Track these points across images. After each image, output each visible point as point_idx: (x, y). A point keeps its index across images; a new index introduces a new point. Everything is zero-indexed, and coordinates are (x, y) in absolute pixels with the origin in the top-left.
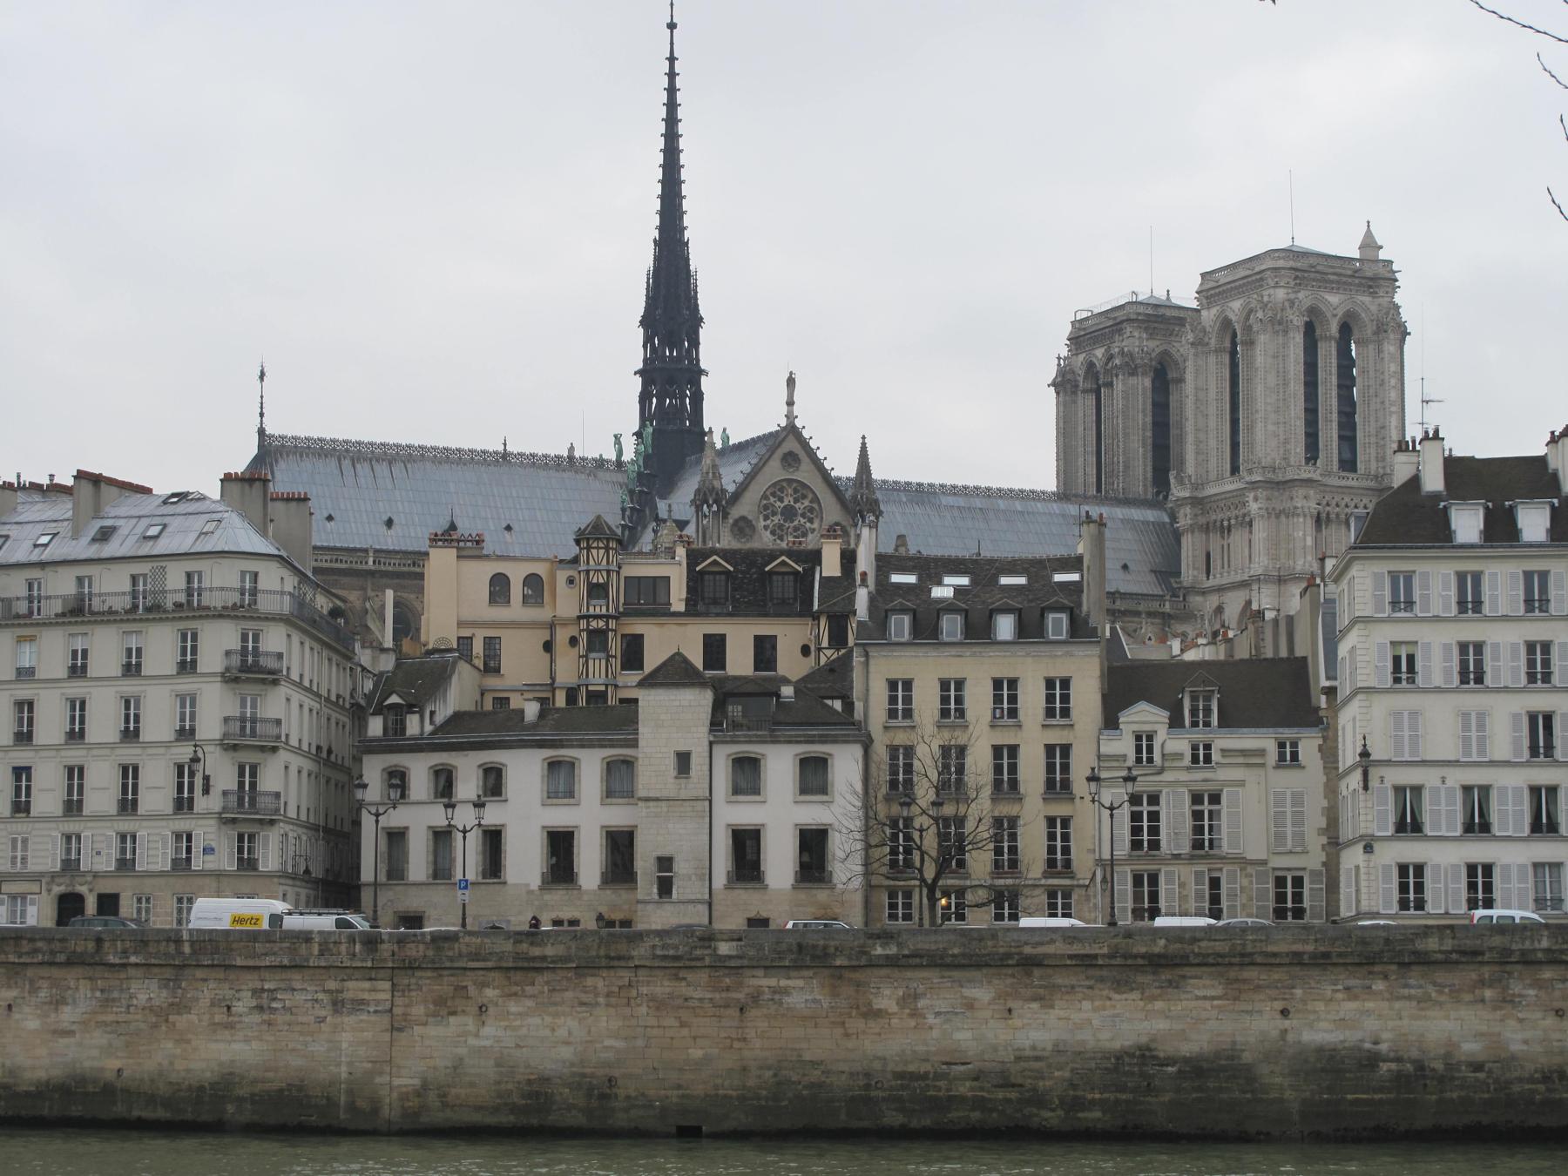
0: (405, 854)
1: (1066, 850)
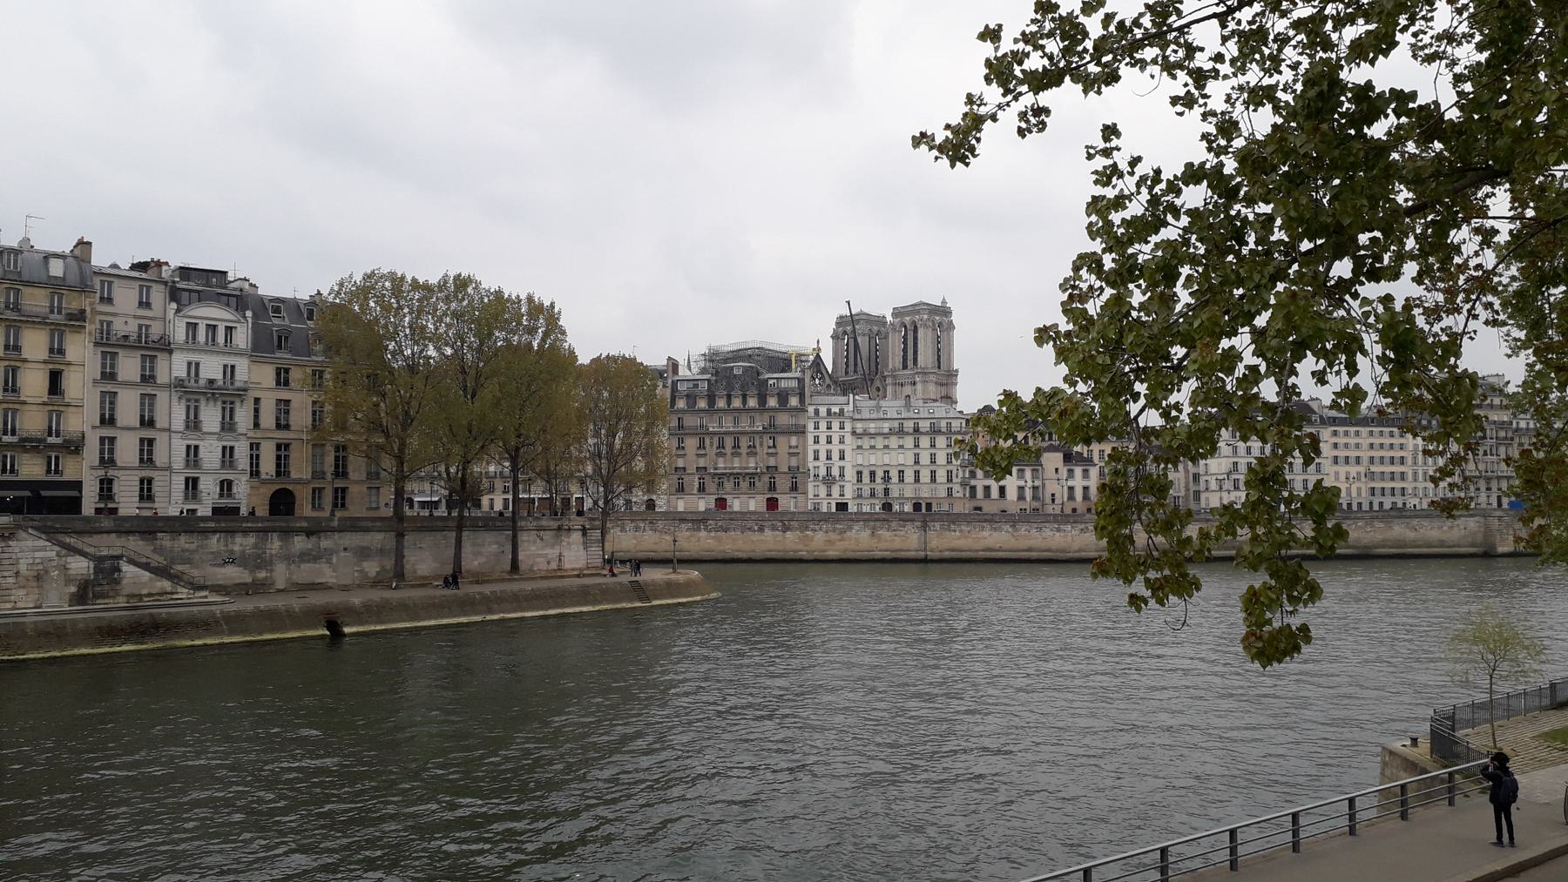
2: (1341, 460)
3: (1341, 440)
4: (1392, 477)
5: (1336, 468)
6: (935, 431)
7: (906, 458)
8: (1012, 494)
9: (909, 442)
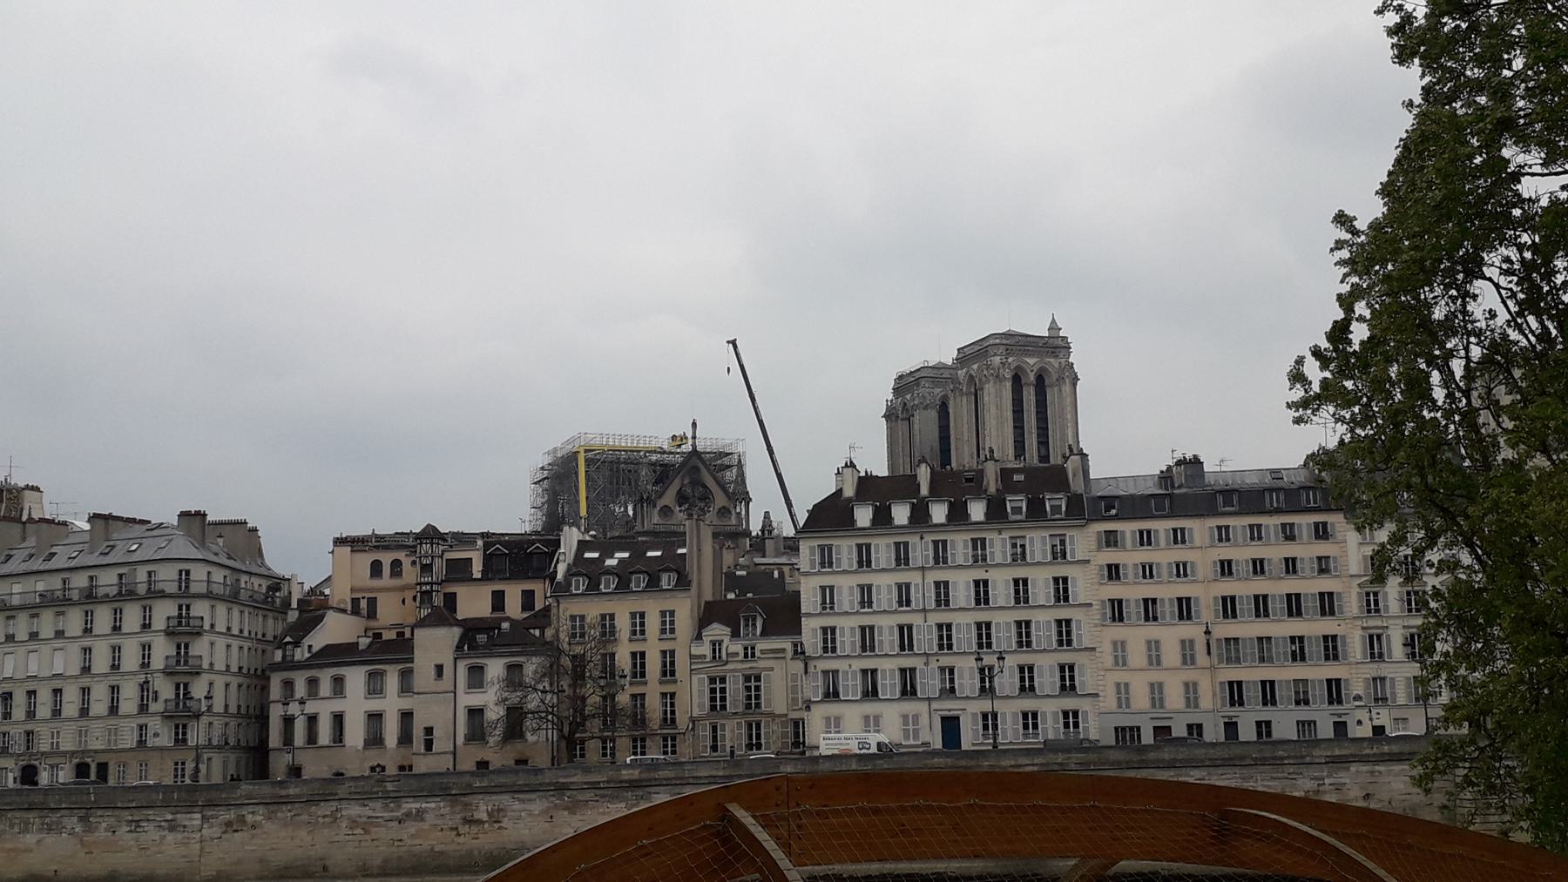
0: (292, 734)
1: (673, 712)
2: (1133, 611)
3: (1130, 558)
4: (1298, 650)
5: (1118, 631)
6: (126, 594)
7: (65, 661)
8: (355, 734)
9: (74, 621)
